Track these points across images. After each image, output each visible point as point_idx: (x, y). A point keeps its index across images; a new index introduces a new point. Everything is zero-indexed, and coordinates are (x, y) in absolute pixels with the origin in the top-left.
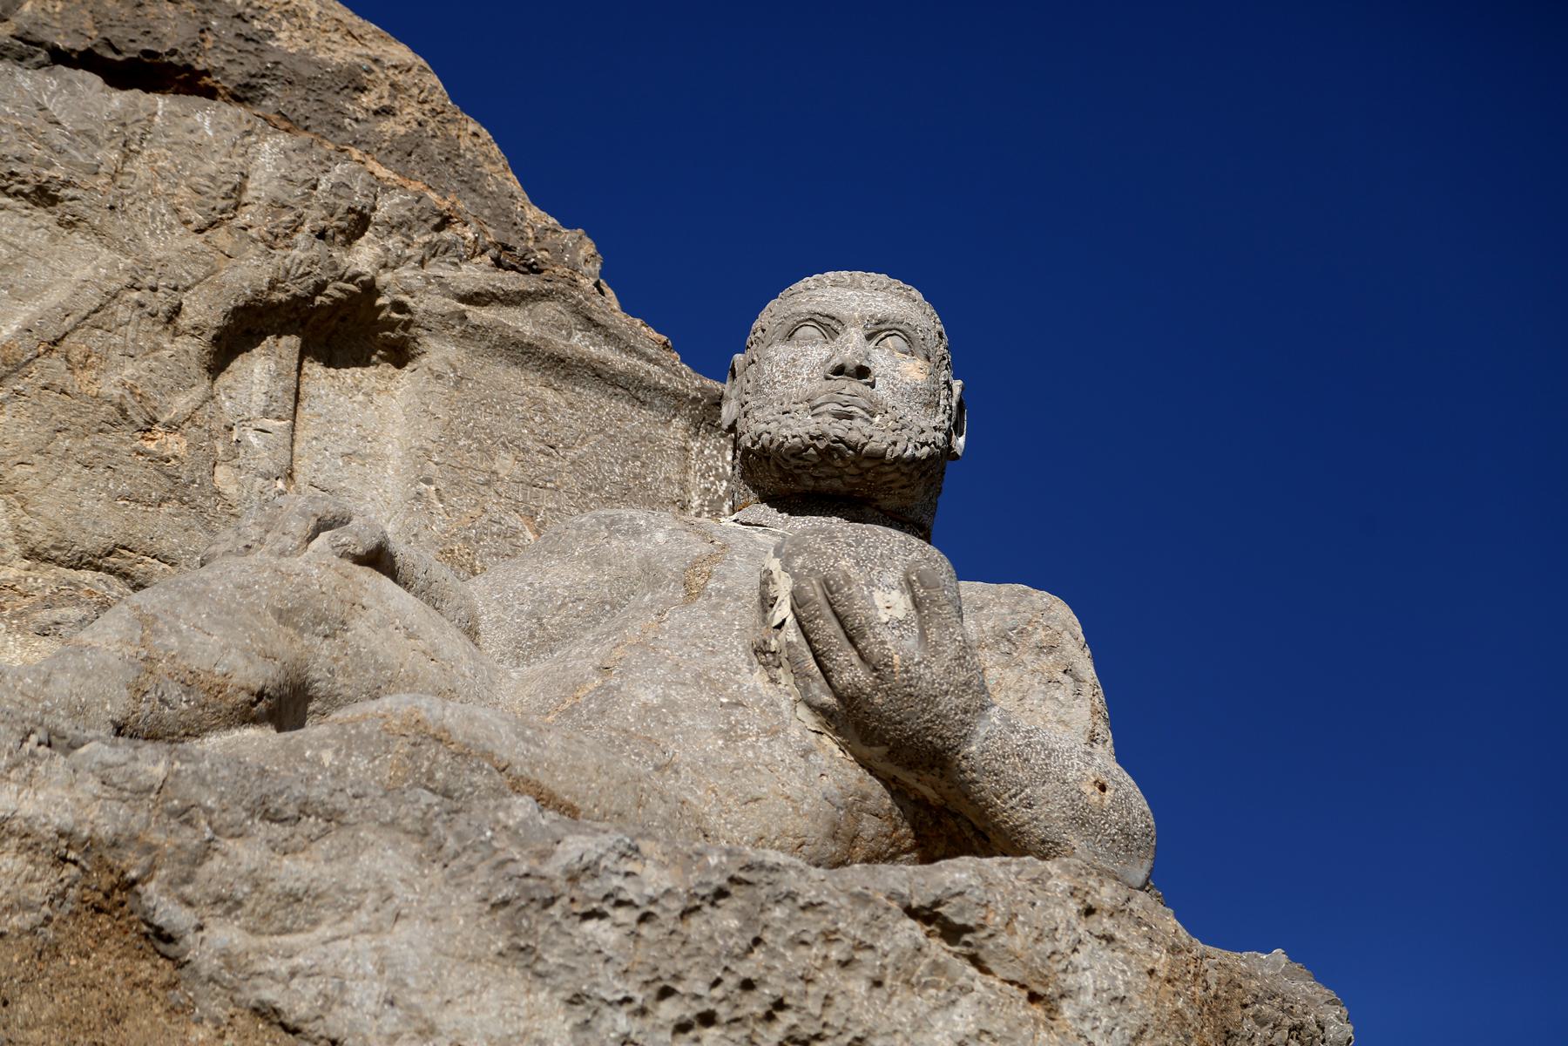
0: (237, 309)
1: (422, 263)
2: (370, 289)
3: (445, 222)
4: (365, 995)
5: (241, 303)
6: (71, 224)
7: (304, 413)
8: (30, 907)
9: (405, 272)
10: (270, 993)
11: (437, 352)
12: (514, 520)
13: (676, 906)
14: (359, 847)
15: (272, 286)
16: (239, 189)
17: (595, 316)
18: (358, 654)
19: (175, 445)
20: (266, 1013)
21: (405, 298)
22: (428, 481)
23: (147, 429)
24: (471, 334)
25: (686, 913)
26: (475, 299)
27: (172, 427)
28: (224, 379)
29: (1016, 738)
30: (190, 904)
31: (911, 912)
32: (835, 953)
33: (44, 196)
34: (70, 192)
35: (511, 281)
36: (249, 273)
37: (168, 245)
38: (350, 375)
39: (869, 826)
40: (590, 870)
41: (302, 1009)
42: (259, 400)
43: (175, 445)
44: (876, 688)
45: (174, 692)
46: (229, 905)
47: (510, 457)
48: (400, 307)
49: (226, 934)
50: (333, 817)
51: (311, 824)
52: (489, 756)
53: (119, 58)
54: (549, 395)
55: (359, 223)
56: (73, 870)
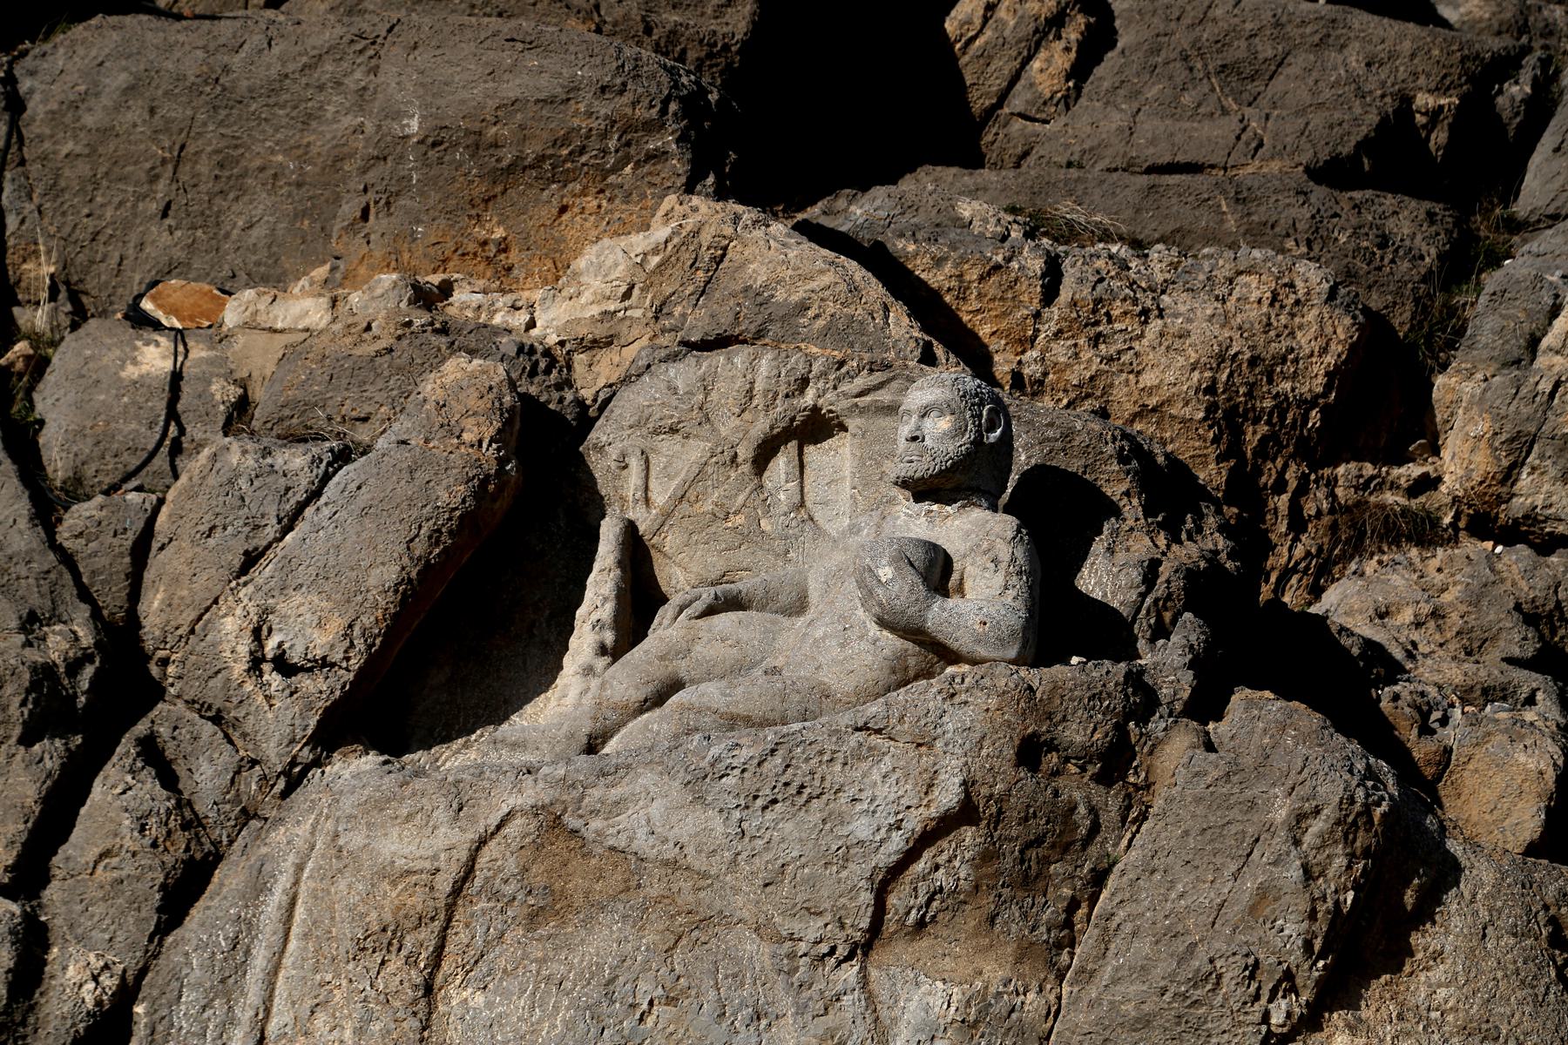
0: (759, 446)
1: (835, 388)
2: (815, 409)
3: (841, 364)
4: (641, 834)
7: (807, 471)
8: (529, 834)
9: (828, 396)
10: (611, 842)
11: (853, 423)
13: (756, 761)
14: (638, 776)
15: (772, 428)
16: (750, 390)
20: (613, 849)
23: (726, 518)
24: (863, 411)
25: (759, 764)
26: (861, 394)
27: (735, 513)
28: (767, 474)
29: (945, 614)
32: (826, 758)
33: (673, 430)
35: (878, 377)
36: (761, 426)
37: (727, 426)
38: (825, 444)
39: (912, 661)
40: (717, 760)
41: (623, 844)
42: (783, 476)
43: (740, 520)
46: (595, 812)
48: (830, 411)
49: (596, 824)
50: (628, 766)
51: (622, 772)
52: (709, 709)
55: (804, 383)
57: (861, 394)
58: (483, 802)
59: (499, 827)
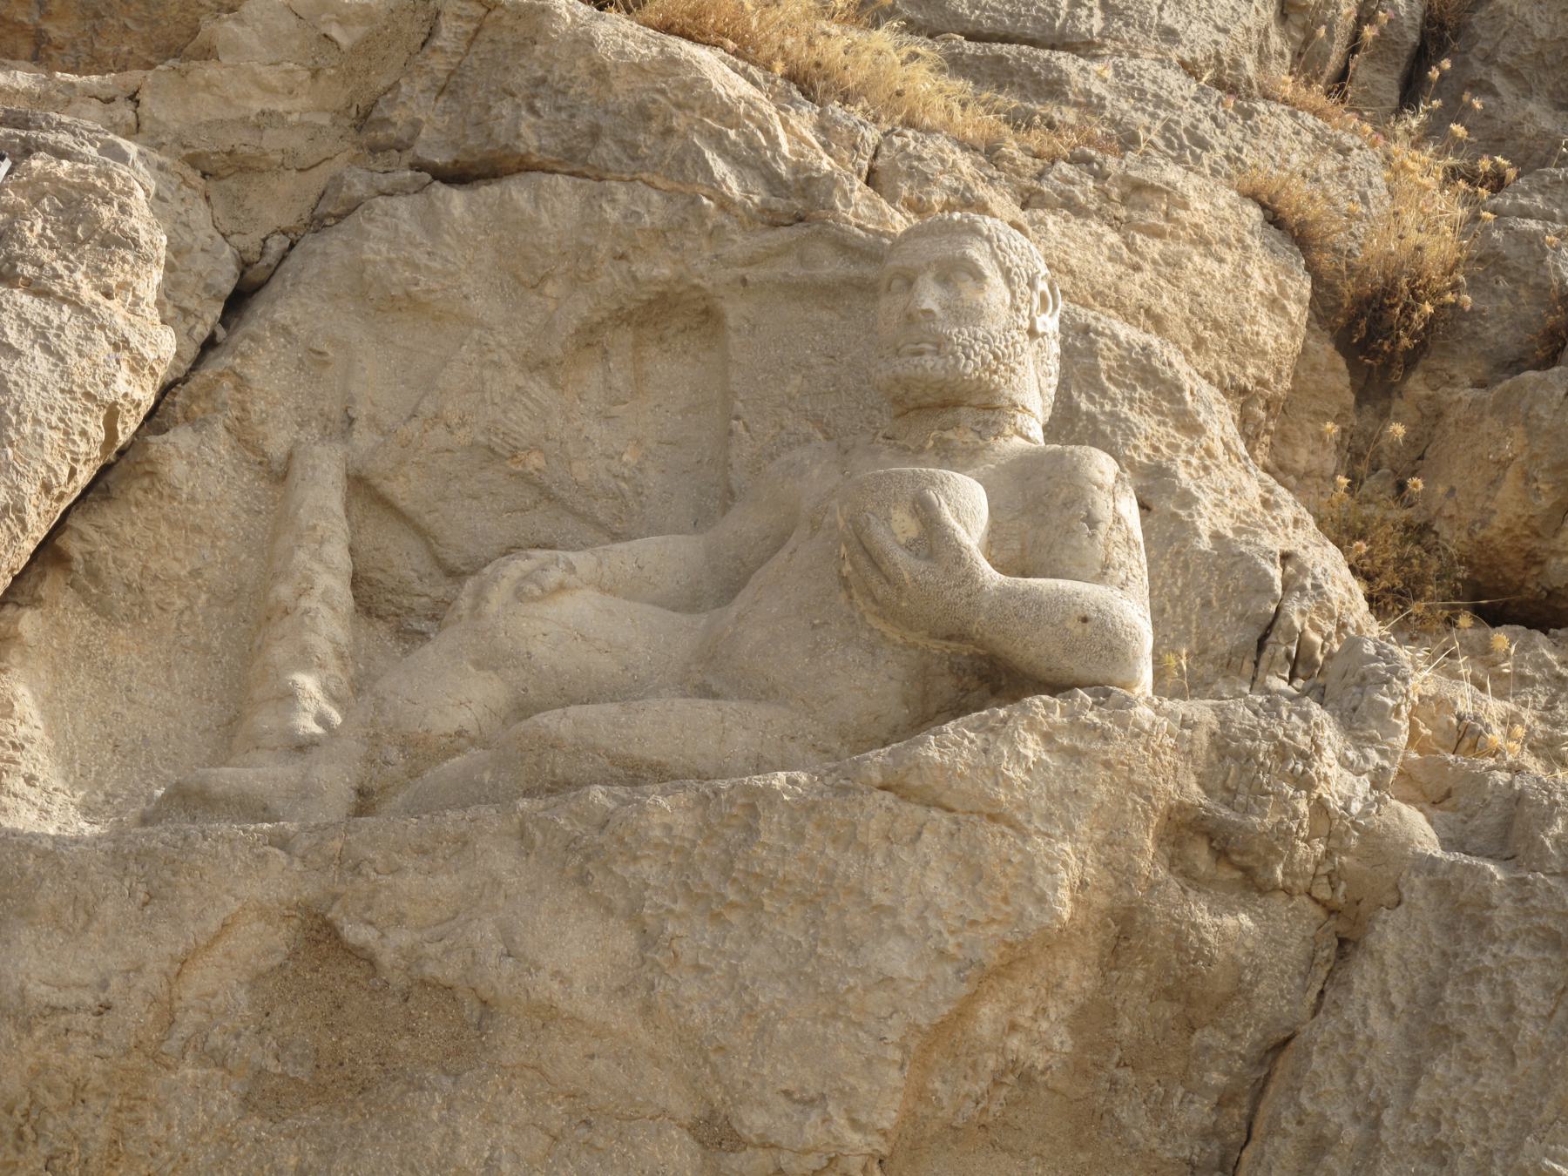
5: (572, 331)
6: (440, 318)
10: (431, 969)
11: (735, 311)
12: (807, 428)
17: (849, 241)
18: (541, 671)
19: (535, 461)
21: (696, 281)
22: (737, 418)
26: (751, 262)
30: (371, 923)
31: (883, 788)
34: (432, 297)
44: (899, 597)
45: (393, 754)
47: (799, 377)
48: (696, 287)
53: (476, 159)
54: (826, 316)
56: (296, 921)
57: (751, 262)
58: (188, 892)
59: (217, 937)
